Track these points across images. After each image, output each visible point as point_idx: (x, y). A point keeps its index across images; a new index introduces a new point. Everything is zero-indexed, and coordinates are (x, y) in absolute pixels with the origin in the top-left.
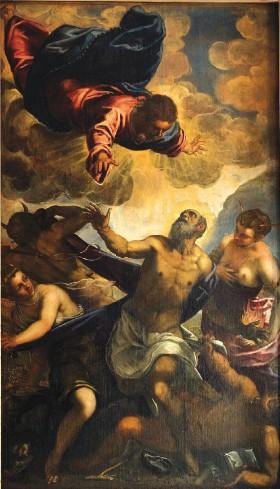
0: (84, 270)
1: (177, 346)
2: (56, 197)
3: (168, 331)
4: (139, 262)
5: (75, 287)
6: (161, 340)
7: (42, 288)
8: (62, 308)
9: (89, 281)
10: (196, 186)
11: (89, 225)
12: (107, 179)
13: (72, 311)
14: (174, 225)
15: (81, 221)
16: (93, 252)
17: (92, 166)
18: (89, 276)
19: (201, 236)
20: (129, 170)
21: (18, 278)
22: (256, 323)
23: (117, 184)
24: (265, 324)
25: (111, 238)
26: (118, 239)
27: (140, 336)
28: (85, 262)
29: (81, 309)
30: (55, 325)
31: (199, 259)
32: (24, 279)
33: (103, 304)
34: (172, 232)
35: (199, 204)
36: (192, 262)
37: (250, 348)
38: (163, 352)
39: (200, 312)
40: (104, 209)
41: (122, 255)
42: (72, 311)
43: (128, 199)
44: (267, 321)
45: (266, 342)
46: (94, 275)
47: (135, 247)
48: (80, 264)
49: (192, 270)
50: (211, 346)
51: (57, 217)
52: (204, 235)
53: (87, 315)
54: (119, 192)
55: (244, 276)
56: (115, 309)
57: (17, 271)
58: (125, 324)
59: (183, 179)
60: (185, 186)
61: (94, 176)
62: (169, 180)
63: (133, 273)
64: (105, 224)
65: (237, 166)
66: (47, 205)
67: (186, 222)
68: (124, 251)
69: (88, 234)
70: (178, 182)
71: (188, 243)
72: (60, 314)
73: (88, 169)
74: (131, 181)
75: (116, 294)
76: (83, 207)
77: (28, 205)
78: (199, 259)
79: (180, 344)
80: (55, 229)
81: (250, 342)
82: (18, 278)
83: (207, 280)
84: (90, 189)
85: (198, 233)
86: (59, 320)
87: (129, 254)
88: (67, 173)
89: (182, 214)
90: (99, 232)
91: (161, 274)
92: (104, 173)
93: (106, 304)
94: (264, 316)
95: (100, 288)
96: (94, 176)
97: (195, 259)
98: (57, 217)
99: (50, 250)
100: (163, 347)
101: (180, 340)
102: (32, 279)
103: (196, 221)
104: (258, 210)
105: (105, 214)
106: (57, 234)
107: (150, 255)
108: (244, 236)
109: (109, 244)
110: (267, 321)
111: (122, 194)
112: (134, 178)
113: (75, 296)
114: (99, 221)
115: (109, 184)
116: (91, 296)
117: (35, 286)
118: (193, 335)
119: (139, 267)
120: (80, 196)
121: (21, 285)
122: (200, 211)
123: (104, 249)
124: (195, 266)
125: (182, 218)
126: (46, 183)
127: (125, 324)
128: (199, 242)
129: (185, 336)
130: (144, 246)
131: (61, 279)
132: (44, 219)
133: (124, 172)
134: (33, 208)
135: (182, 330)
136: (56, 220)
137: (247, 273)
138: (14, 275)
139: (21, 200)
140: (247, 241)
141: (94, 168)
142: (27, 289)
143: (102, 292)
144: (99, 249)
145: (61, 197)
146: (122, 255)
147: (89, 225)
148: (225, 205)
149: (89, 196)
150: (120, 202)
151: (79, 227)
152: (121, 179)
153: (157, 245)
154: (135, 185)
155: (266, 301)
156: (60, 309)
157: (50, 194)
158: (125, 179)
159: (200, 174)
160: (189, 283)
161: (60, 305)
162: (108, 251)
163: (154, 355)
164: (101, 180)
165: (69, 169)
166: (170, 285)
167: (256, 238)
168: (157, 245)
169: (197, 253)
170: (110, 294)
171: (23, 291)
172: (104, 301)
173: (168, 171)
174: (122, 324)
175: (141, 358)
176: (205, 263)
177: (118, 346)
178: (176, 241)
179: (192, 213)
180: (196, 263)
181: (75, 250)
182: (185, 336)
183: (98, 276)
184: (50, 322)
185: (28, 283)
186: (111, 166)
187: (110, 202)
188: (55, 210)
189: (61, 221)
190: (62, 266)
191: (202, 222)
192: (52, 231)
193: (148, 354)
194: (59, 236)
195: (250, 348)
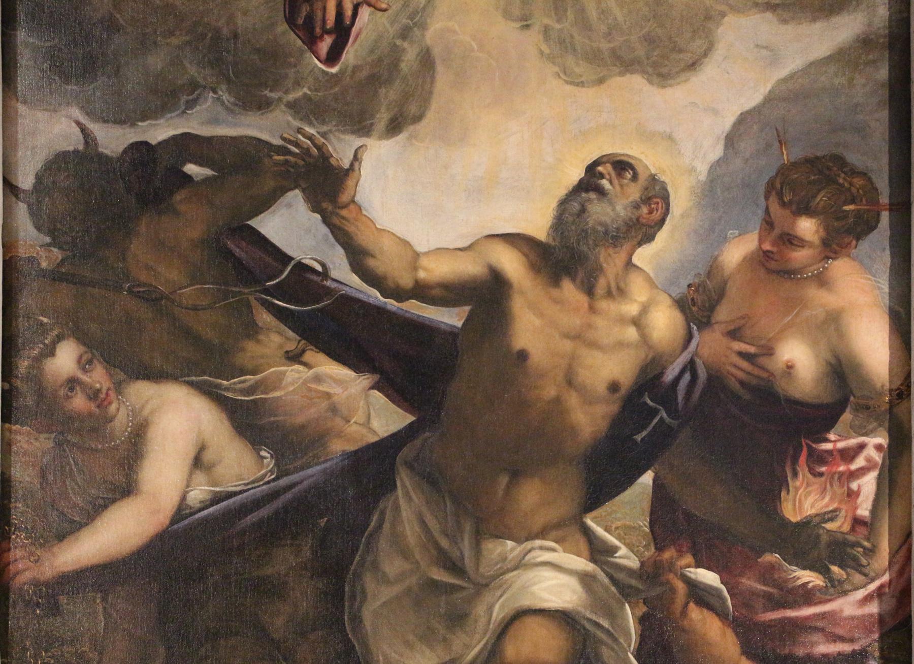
0: (276, 339)
1: (573, 583)
2: (191, 104)
3: (542, 534)
4: (451, 318)
6: (520, 565)
7: (142, 392)
8: (208, 456)
9: (294, 373)
10: (637, 81)
11: (296, 197)
12: (350, 55)
13: (240, 467)
14: (563, 203)
15: (270, 184)
16: (304, 281)
17: (305, 10)
18: (294, 358)
19: (649, 238)
20: (423, 27)
22: (831, 516)
23: (382, 71)
24: (858, 522)
25: (364, 238)
26: (387, 244)
27: (455, 554)
28: (281, 315)
29: (270, 463)
31: (645, 309)
32: (84, 364)
33: (338, 447)
34: (559, 224)
35: (647, 136)
36: (622, 320)
37: (807, 596)
38: (526, 602)
39: (647, 478)
40: (342, 148)
41: (400, 294)
42: (240, 467)
43: (418, 118)
44: (864, 511)
45: (858, 578)
46: (312, 356)
47: (438, 270)
48: (265, 318)
49: (621, 345)
50: (680, 586)
52: (662, 236)
54: (389, 95)
55: (790, 367)
56: (375, 466)
57: (60, 338)
58: (406, 512)
59: (594, 57)
60: (601, 81)
61: (311, 41)
62: (551, 58)
63: (431, 348)
64: (344, 198)
65: (769, 15)
67: (601, 192)
68: (406, 281)
69: (290, 226)
70: (582, 69)
71: (611, 262)
73: (291, 21)
74: (427, 61)
75: (384, 418)
76: (277, 142)
77: (98, 130)
78: (645, 309)
79: (586, 579)
81: (808, 577)
83: (670, 375)
84: (297, 84)
85: (644, 230)
86: (198, 494)
87: (421, 292)
88: (225, 31)
89: (591, 169)
90: (326, 221)
91: (523, 356)
92: (342, 32)
93: (351, 447)
94: (853, 495)
95: (328, 395)
96: (311, 41)
97: (632, 309)
98: (191, 169)
99: (168, 274)
100: (524, 588)
101: (582, 564)
102: (110, 362)
103: (634, 192)
104: (839, 161)
105: (346, 164)
106: (191, 222)
107: (487, 296)
108: (790, 240)
109: (358, 257)
110: (864, 511)
111: (406, 97)
112: (436, 52)
113: (250, 420)
114: (326, 184)
115: (356, 69)
116: (300, 420)
117: (119, 387)
118: (623, 551)
119: (452, 334)
120: (263, 106)
121: (72, 383)
122: (650, 159)
123: (342, 271)
124: (631, 333)
125: (590, 182)
126: (156, 61)
127: (408, 509)
128: (643, 256)
129: (598, 552)
130: (470, 268)
131: (205, 365)
133: (405, 33)
134: (113, 140)
135: (587, 533)
136: (188, 178)
137: (799, 359)
138: (51, 352)
139: (76, 113)
140: (800, 256)
141: (310, 19)
143: (334, 410)
144: (325, 274)
145: (207, 104)
146: (400, 294)
147: (296, 197)
148: (731, 140)
149: (293, 106)
150: (395, 127)
151: (264, 204)
152: (396, 54)
153: (511, 263)
154: (443, 79)
155: (862, 447)
156: (199, 462)
157: (167, 97)
158: (410, 56)
159: (650, 40)
160: (614, 387)
161: (201, 449)
162: (355, 280)
163: (499, 613)
164: (333, 57)
165: (231, 18)
166: (550, 392)
167: (833, 245)
168: (511, 263)
169: (639, 292)
170: (359, 417)
171: (79, 402)
172: (340, 435)
173: (546, 30)
174: (397, 508)
175: (458, 619)
176: (664, 322)
177: (386, 581)
178: (568, 255)
179: (622, 166)
180: (636, 322)
181: (246, 275)
182: (598, 552)
184: (168, 503)
185: (98, 377)
186: (365, 13)
187: (361, 125)
188: (187, 146)
191: (656, 196)
193: (480, 609)
194: (195, 232)
195: (807, 596)
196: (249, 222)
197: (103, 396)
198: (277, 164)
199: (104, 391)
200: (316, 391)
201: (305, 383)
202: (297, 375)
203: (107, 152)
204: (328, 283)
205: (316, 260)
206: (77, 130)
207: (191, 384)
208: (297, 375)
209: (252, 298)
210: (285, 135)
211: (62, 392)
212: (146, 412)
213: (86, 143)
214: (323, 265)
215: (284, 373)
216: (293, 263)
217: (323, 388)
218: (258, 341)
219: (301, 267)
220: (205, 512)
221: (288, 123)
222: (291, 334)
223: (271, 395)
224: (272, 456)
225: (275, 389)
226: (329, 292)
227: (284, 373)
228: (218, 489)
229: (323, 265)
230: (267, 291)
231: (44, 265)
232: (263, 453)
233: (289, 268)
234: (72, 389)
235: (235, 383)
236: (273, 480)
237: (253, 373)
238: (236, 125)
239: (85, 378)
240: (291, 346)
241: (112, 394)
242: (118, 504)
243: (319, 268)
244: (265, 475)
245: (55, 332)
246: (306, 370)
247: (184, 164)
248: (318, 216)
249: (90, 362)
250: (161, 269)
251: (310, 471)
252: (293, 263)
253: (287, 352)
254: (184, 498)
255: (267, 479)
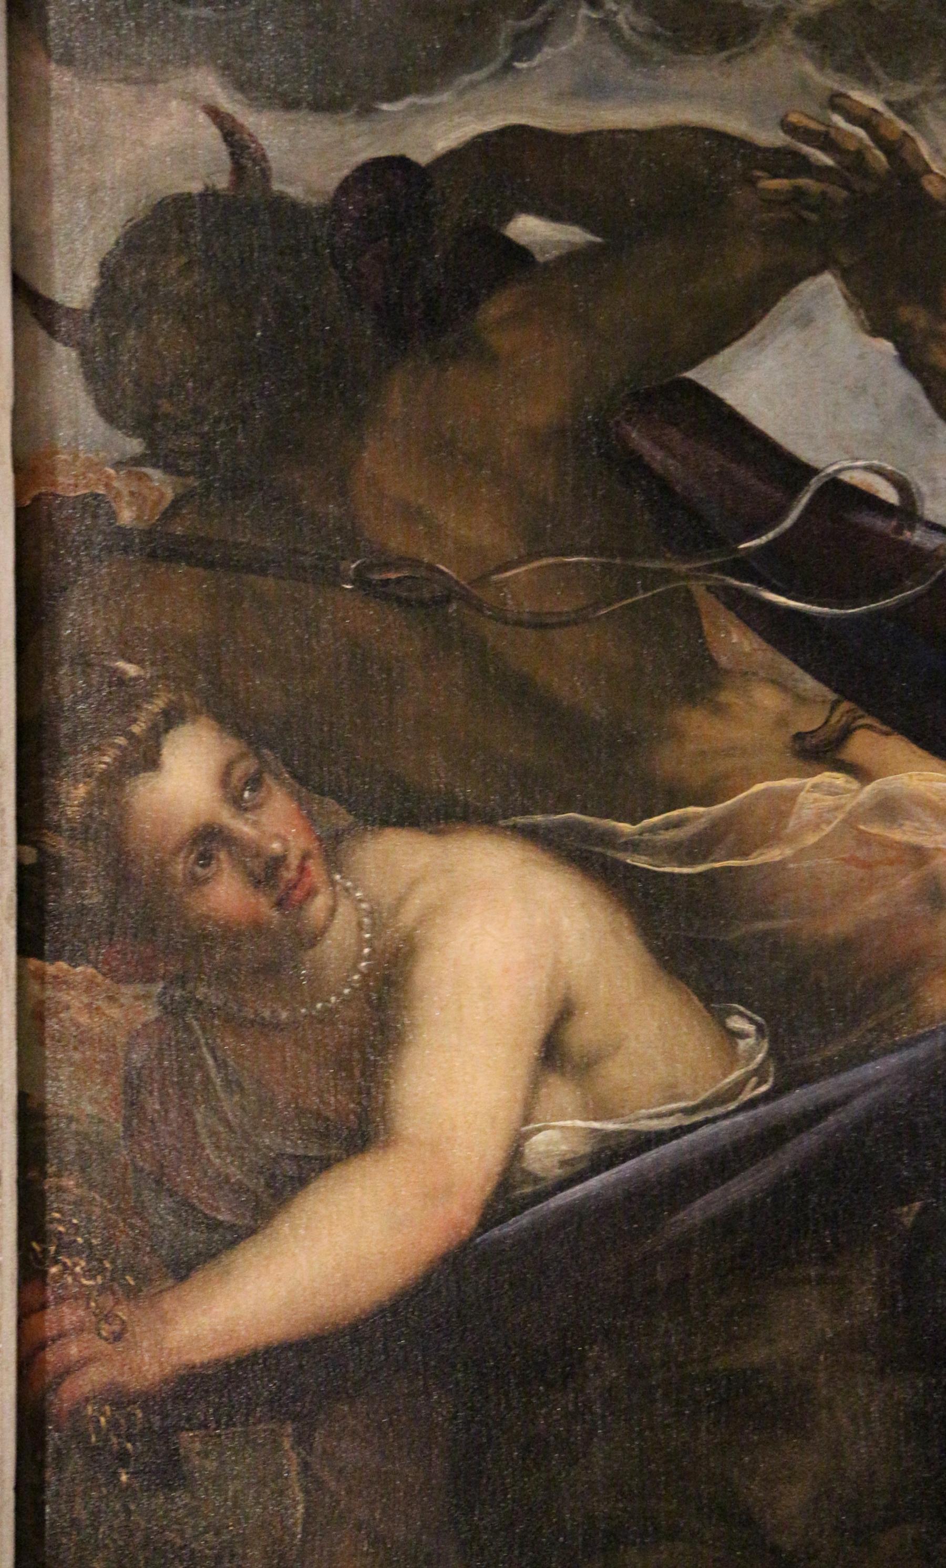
0: (768, 699)
2: (527, 44)
5: (701, 845)
7: (397, 860)
8: (583, 1034)
9: (820, 794)
11: (824, 294)
13: (669, 1060)
15: (748, 259)
18: (820, 751)
21: (187, 776)
28: (782, 631)
29: (753, 1048)
30: (511, 1190)
32: (237, 790)
42: (669, 1060)
46: (866, 744)
48: (736, 642)
51: (528, 228)
53: (796, 1101)
57: (171, 719)
66: (439, 128)
72: (561, 1093)
77: (267, 129)
80: (502, 341)
82: (187, 776)
86: (555, 1141)
98: (528, 228)
99: (465, 531)
102: (307, 781)
106: (528, 381)
113: (694, 931)
116: (839, 925)
117: (333, 849)
121: (208, 840)
131: (567, 781)
132: (416, 254)
134: (310, 156)
136: (519, 256)
139: (210, 85)
142: (266, 873)
144: (908, 511)
147: (824, 294)
151: (733, 319)
156: (556, 1051)
161: (563, 1015)
171: (227, 894)
181: (686, 525)
183: (897, 748)
185: (278, 823)
188: (513, 164)
189: (573, 258)
190: (574, 666)
192: (488, 359)
196: (690, 375)
197: (289, 874)
198: (771, 201)
199: (294, 861)
200: (887, 844)
201: (851, 821)
202: (830, 801)
203: (295, 191)
204: (917, 536)
205: (880, 472)
206: (211, 134)
207: (531, 835)
208: (830, 801)
209: (698, 588)
210: (794, 118)
211: (179, 868)
212: (408, 916)
213: (238, 170)
214: (902, 486)
215: (791, 796)
216: (815, 483)
217: (903, 834)
218: (719, 710)
219: (841, 496)
220: (577, 1192)
221: (804, 85)
222: (809, 684)
223: (755, 859)
224: (760, 1029)
225: (769, 839)
226: (917, 559)
227: (791, 796)
228: (610, 1126)
229: (902, 486)
230: (743, 567)
231: (126, 516)
232: (737, 1023)
233: (805, 500)
234: (206, 858)
235: (653, 829)
236: (766, 1098)
237: (706, 797)
238: (656, 96)
239: (242, 827)
240: (810, 720)
241: (314, 866)
242: (336, 1173)
243: (890, 495)
244: (740, 1085)
245: (158, 704)
246: (855, 785)
247: (508, 217)
248: (887, 346)
249: (255, 782)
250: (449, 517)
251: (872, 1070)
252: (815, 483)
253: (799, 736)
254: (515, 1153)
255: (746, 1096)
